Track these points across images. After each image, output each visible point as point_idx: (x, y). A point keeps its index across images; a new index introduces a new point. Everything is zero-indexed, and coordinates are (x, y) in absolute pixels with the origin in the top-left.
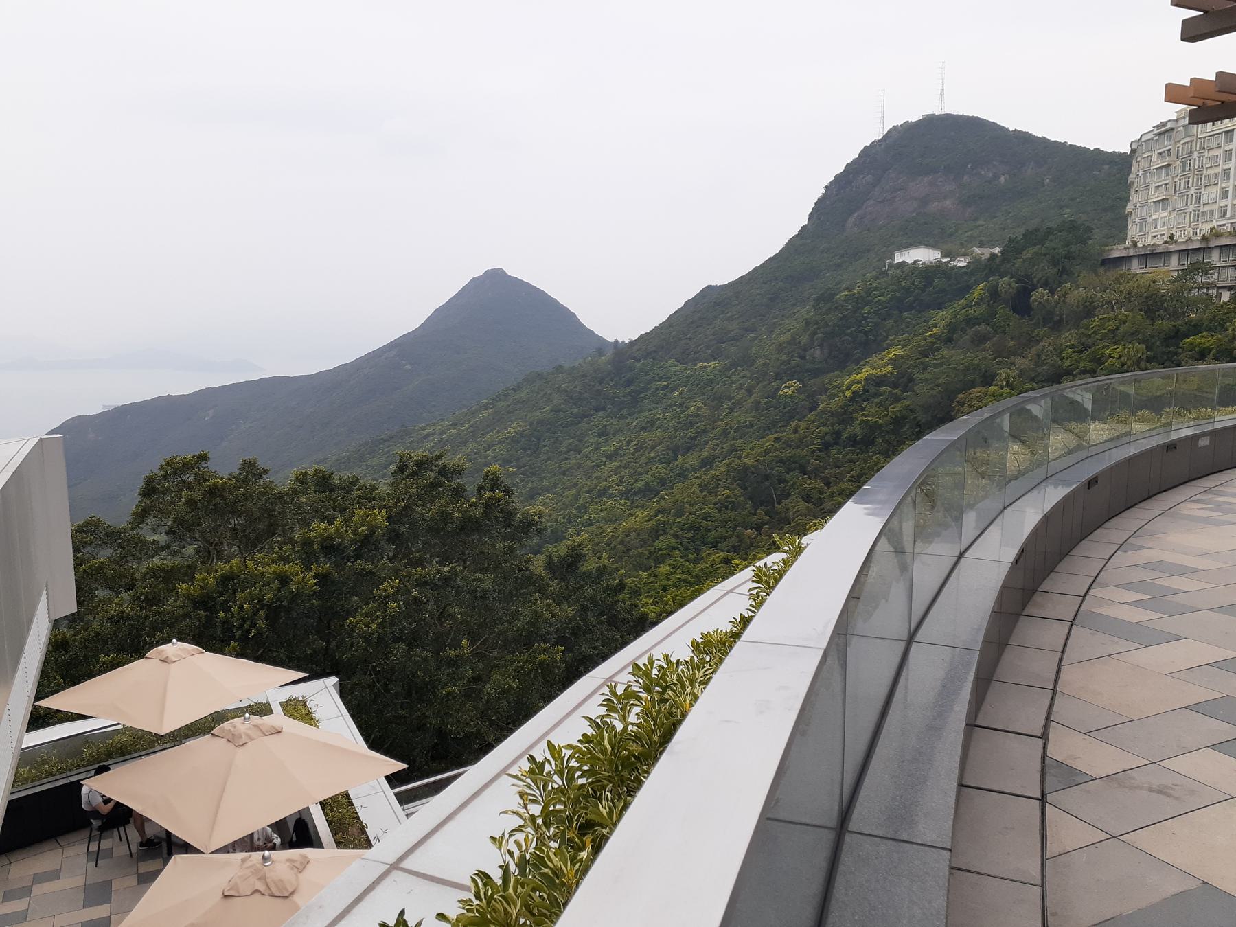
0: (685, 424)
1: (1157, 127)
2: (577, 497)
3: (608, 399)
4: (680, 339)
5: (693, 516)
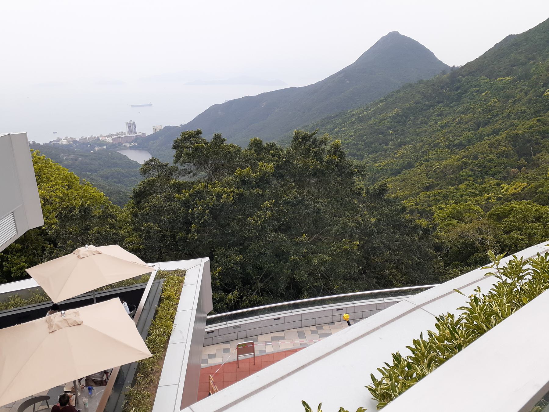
0: (486, 111)
2: (422, 147)
3: (445, 97)
4: (490, 65)
5: (483, 160)
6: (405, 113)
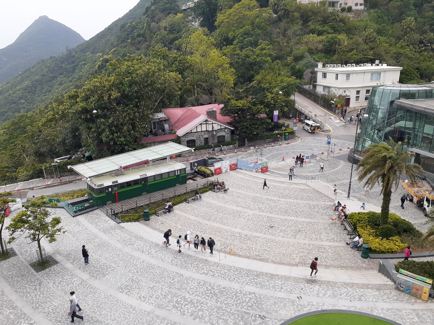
6: (34, 84)
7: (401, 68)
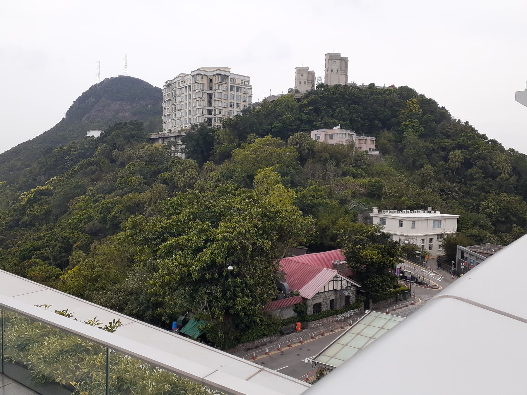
1: (166, 83)
7: (458, 216)
